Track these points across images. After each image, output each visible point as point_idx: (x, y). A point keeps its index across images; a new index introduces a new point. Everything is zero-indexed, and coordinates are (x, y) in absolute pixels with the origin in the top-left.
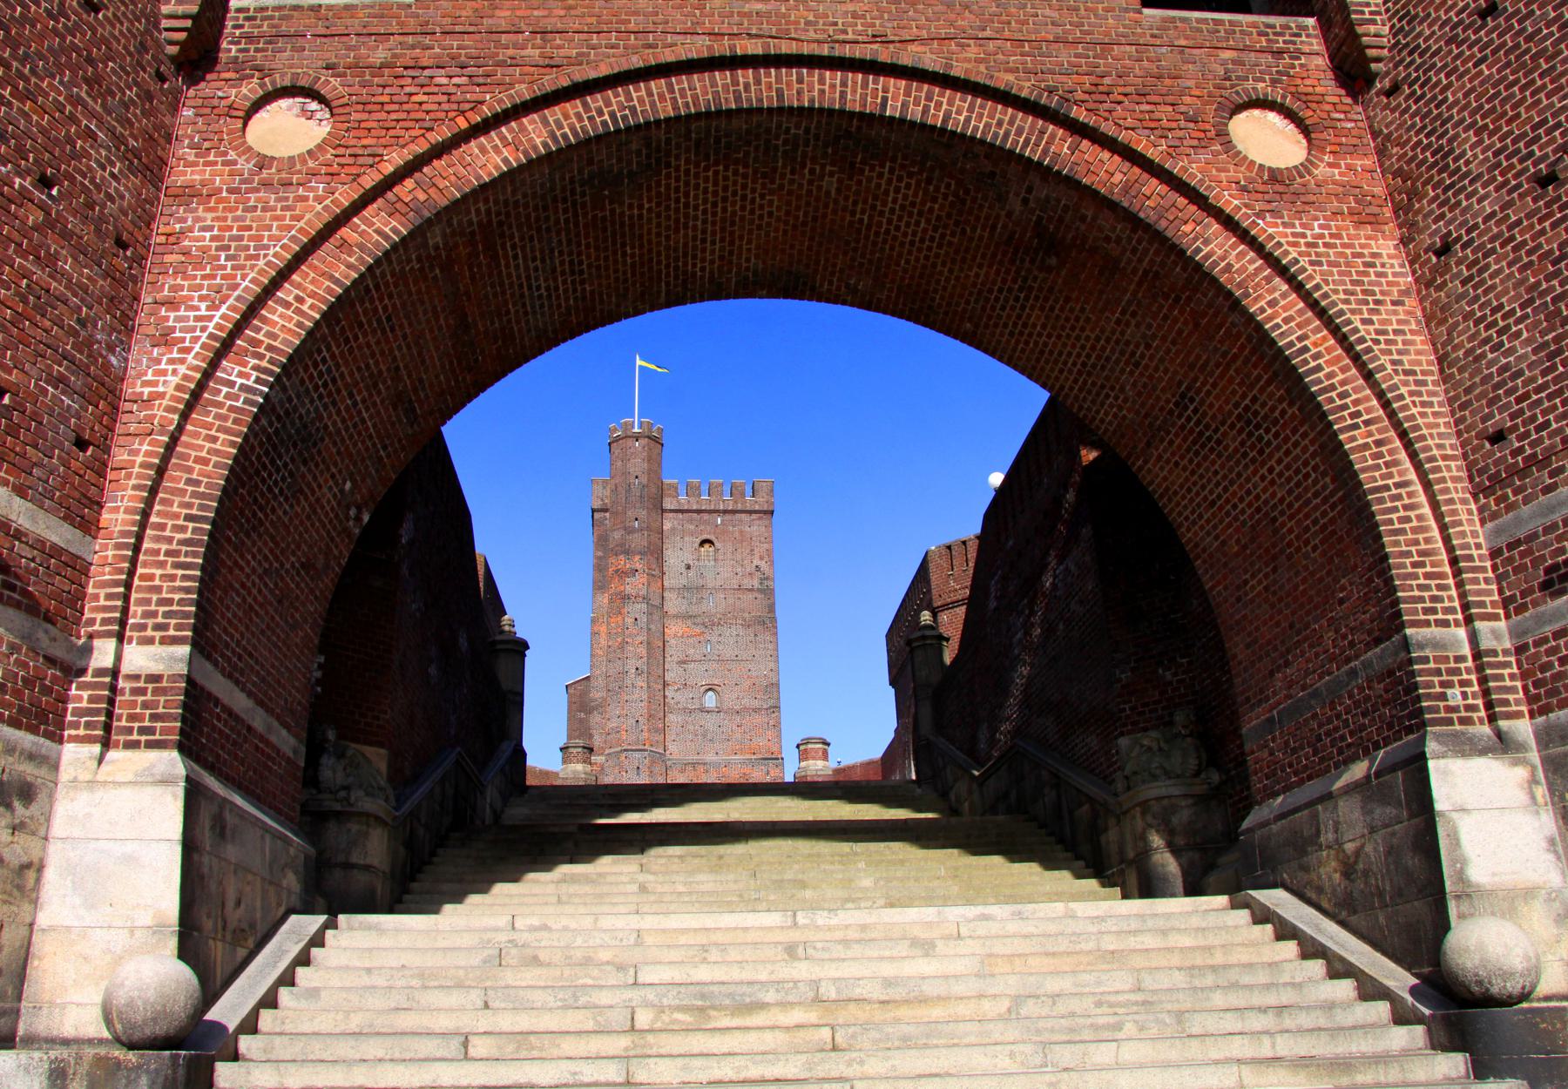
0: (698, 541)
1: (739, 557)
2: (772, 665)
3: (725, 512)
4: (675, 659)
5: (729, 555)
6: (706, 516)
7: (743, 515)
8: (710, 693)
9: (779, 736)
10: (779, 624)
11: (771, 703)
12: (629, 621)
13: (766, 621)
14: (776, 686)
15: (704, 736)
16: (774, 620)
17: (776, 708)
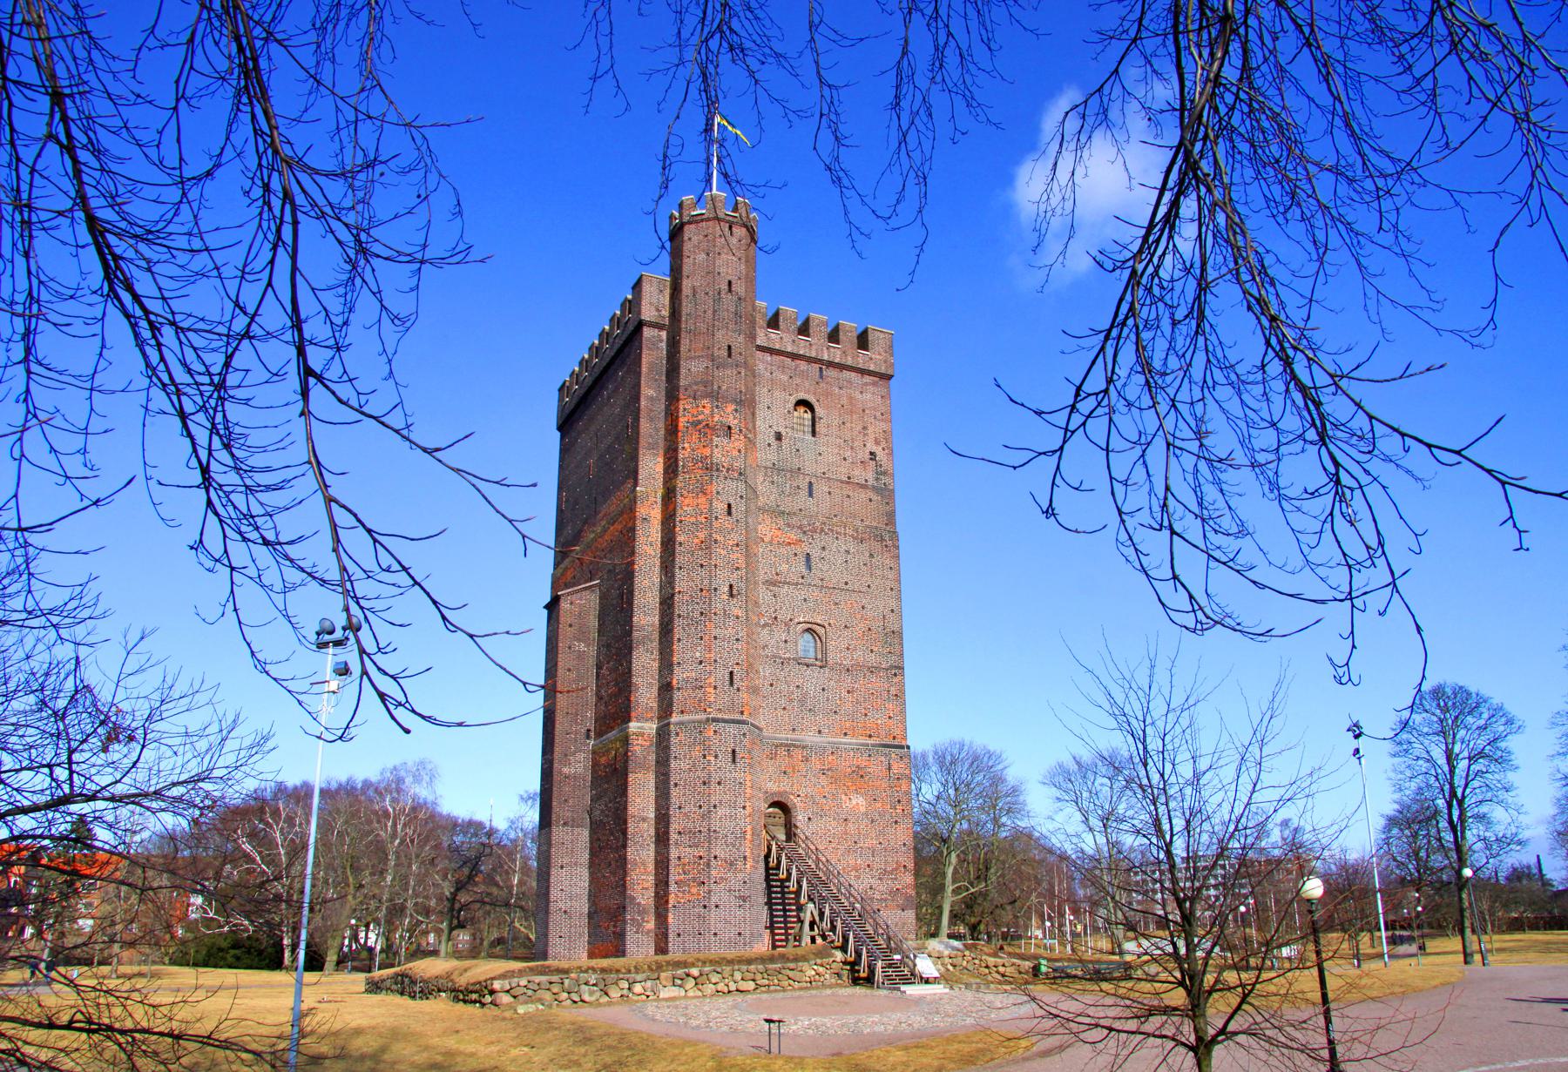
0: (793, 400)
1: (848, 436)
2: (893, 604)
3: (831, 364)
4: (761, 577)
5: (834, 430)
6: (803, 365)
7: (853, 374)
8: (808, 636)
9: (903, 712)
10: (901, 543)
11: (892, 660)
12: (720, 507)
13: (885, 536)
14: (898, 634)
15: (802, 702)
16: (894, 535)
17: (898, 669)
